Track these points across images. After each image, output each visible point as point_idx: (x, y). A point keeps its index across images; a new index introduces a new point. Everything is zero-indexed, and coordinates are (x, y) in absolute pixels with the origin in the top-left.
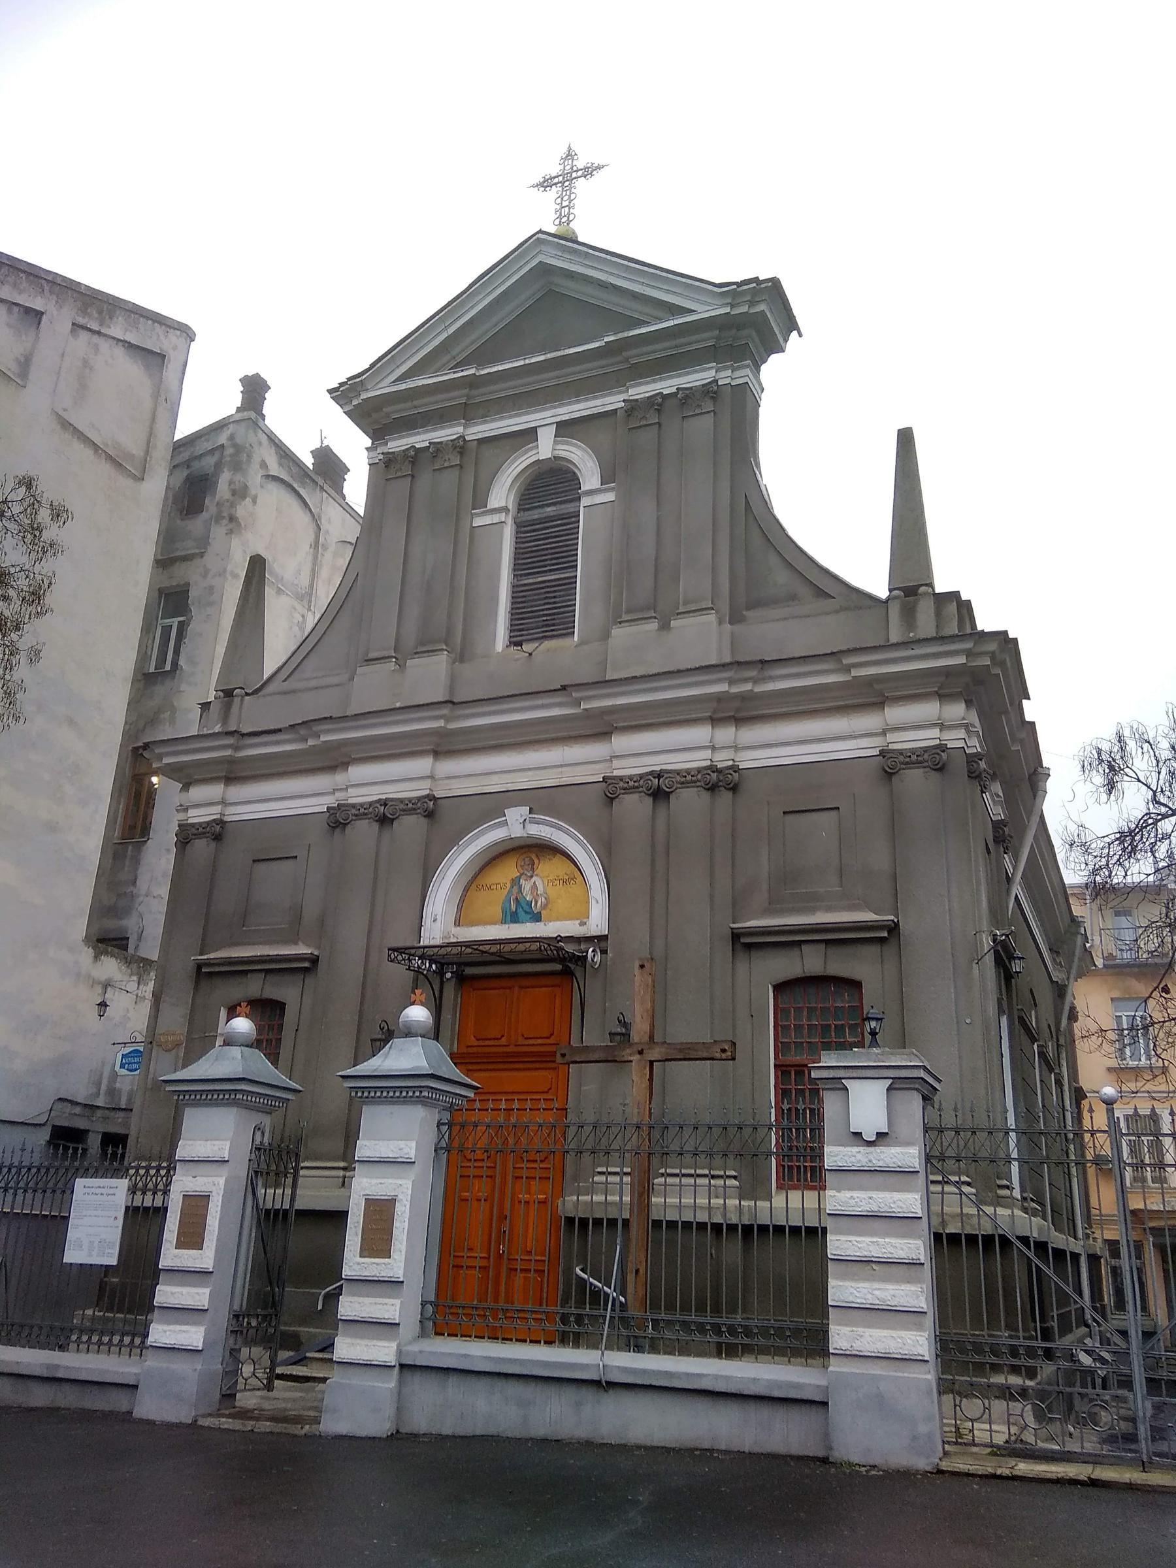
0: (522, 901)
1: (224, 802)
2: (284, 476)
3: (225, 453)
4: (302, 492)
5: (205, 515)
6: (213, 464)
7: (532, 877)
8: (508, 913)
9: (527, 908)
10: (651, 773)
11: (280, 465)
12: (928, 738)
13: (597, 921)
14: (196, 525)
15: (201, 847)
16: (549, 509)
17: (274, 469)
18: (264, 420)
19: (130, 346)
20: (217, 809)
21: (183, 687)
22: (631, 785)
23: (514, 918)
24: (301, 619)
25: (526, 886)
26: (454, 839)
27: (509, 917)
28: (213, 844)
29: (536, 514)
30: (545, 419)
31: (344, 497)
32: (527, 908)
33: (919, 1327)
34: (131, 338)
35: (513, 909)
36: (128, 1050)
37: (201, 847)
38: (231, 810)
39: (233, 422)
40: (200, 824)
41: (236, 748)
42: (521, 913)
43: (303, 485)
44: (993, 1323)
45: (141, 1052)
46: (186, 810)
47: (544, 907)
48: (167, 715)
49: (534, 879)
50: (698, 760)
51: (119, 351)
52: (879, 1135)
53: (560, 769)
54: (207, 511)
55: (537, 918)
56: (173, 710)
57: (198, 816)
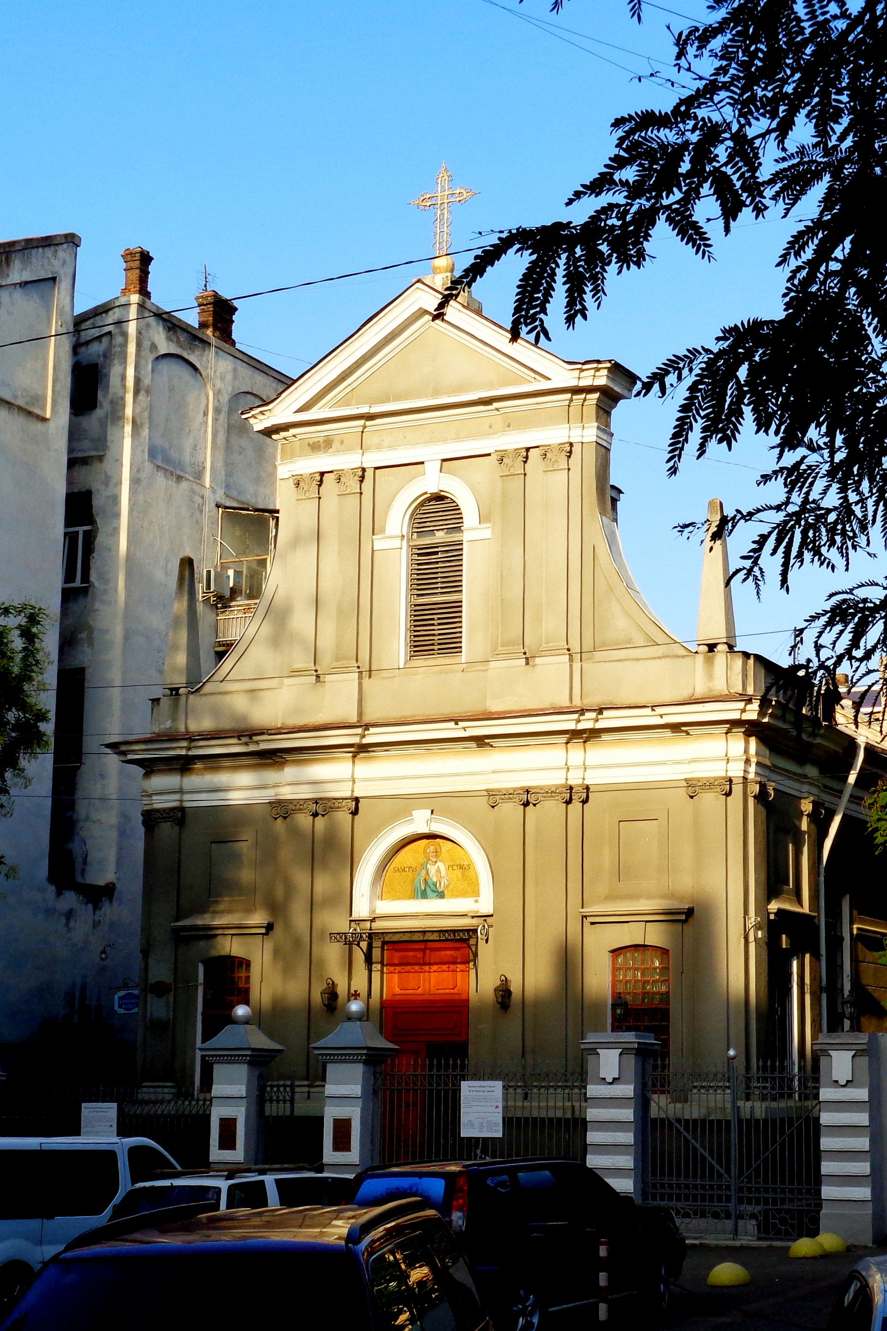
0: (430, 882)
1: (181, 791)
2: (174, 349)
3: (113, 342)
4: (192, 358)
5: (99, 413)
6: (101, 352)
7: (436, 862)
8: (419, 891)
9: (433, 887)
10: (521, 788)
11: (169, 339)
12: (717, 770)
13: (485, 904)
14: (92, 421)
15: (166, 829)
16: (438, 534)
17: (165, 346)
18: (149, 298)
19: (24, 284)
20: (177, 797)
21: (97, 605)
22: (508, 795)
23: (424, 895)
24: (200, 501)
25: (432, 869)
26: (375, 832)
27: (420, 895)
28: (176, 828)
29: (427, 541)
30: (432, 453)
31: (233, 343)
32: (433, 887)
33: (628, 1177)
34: (27, 276)
35: (423, 888)
36: (122, 993)
37: (166, 829)
38: (187, 797)
39: (119, 306)
40: (164, 810)
41: (189, 749)
42: (429, 891)
43: (192, 349)
44: (695, 1176)
45: (136, 997)
46: (150, 795)
47: (447, 887)
48: (84, 635)
49: (439, 864)
50: (556, 779)
51: (18, 294)
52: (614, 1079)
53: (453, 778)
54: (102, 407)
55: (441, 895)
56: (90, 630)
57: (162, 803)
